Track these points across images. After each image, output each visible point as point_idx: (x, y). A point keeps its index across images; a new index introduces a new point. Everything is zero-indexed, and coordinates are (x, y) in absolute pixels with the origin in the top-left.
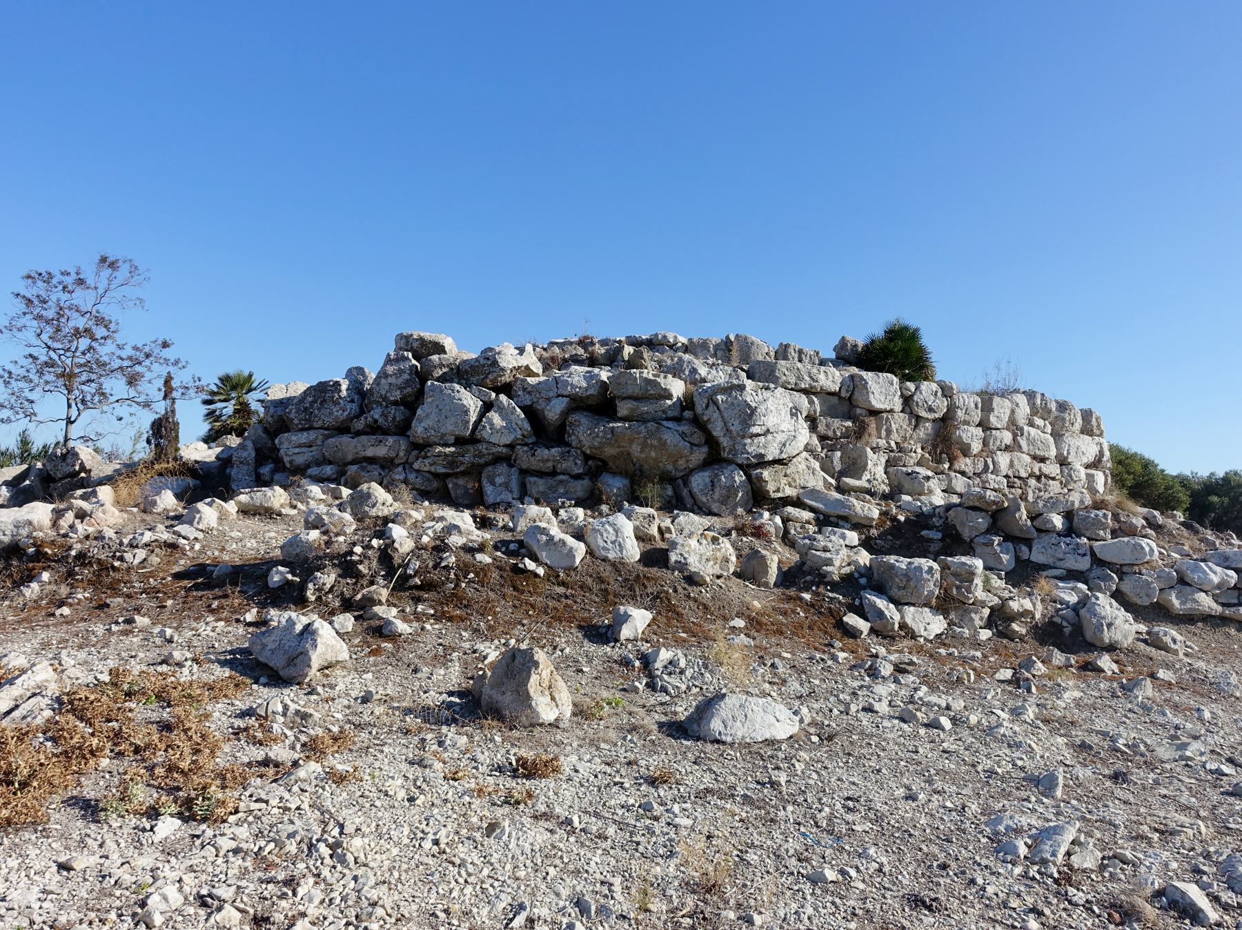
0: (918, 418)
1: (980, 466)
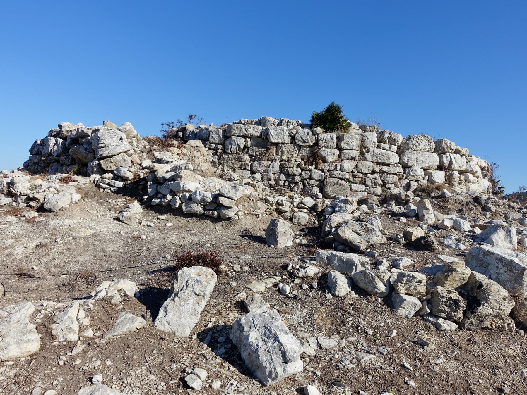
0: (300, 146)
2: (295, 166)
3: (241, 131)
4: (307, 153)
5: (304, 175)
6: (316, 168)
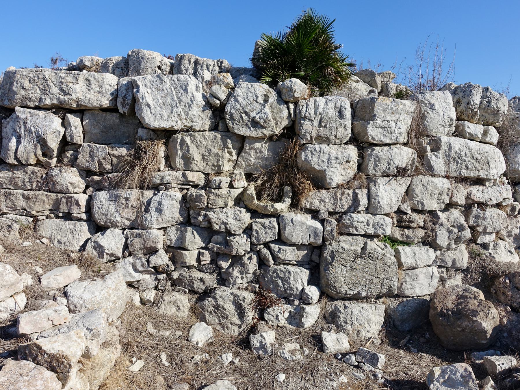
0: (243, 139)
1: (346, 203)
2: (231, 203)
3: (45, 91)
4: (262, 158)
5: (262, 231)
6: (294, 205)
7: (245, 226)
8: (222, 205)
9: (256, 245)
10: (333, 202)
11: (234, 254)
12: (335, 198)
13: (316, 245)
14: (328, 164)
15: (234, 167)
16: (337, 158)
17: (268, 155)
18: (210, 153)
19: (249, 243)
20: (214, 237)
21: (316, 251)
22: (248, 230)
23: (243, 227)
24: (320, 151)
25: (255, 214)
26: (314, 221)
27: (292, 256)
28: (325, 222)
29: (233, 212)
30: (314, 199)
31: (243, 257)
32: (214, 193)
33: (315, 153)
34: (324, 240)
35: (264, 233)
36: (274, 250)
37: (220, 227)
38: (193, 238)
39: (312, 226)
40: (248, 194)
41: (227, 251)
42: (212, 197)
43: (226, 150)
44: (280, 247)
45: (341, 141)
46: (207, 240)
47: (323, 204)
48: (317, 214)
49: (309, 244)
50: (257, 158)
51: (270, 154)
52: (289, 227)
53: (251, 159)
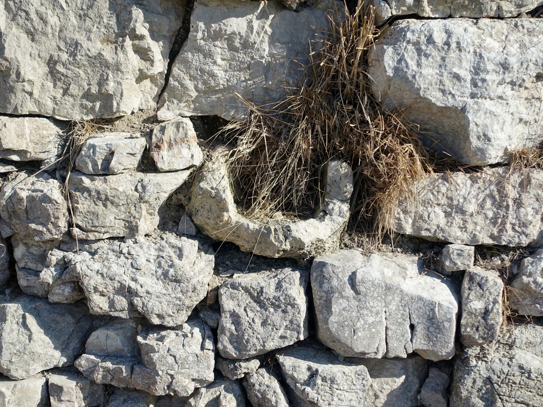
2: (148, 222)
4: (253, 67)
5: (251, 316)
6: (363, 225)
7: (195, 300)
8: (120, 230)
9: (234, 361)
10: (490, 214)
11: (161, 393)
12: (500, 202)
13: (435, 359)
14: (475, 85)
15: (159, 99)
16: (505, 66)
17: (271, 55)
18: (73, 55)
19: (212, 355)
20: (95, 334)
21: (436, 377)
22: (207, 313)
23: (187, 302)
24: (447, 44)
25: (229, 255)
26: (429, 279)
27: (353, 396)
28: (466, 284)
29: (154, 253)
30: (426, 203)
31: (192, 401)
32: (88, 190)
33: (430, 49)
34: (461, 342)
35: (258, 321)
36: (293, 378)
37: (112, 304)
38: (24, 338)
39: (421, 299)
40: (205, 192)
41: (139, 382)
42: (84, 204)
43: (128, 43)
44: (315, 366)
45: (519, 6)
46: (74, 344)
47: (458, 219)
48: (439, 253)
49: (414, 355)
50: (233, 66)
51: (280, 51)
52: (344, 303)
53: (216, 70)
